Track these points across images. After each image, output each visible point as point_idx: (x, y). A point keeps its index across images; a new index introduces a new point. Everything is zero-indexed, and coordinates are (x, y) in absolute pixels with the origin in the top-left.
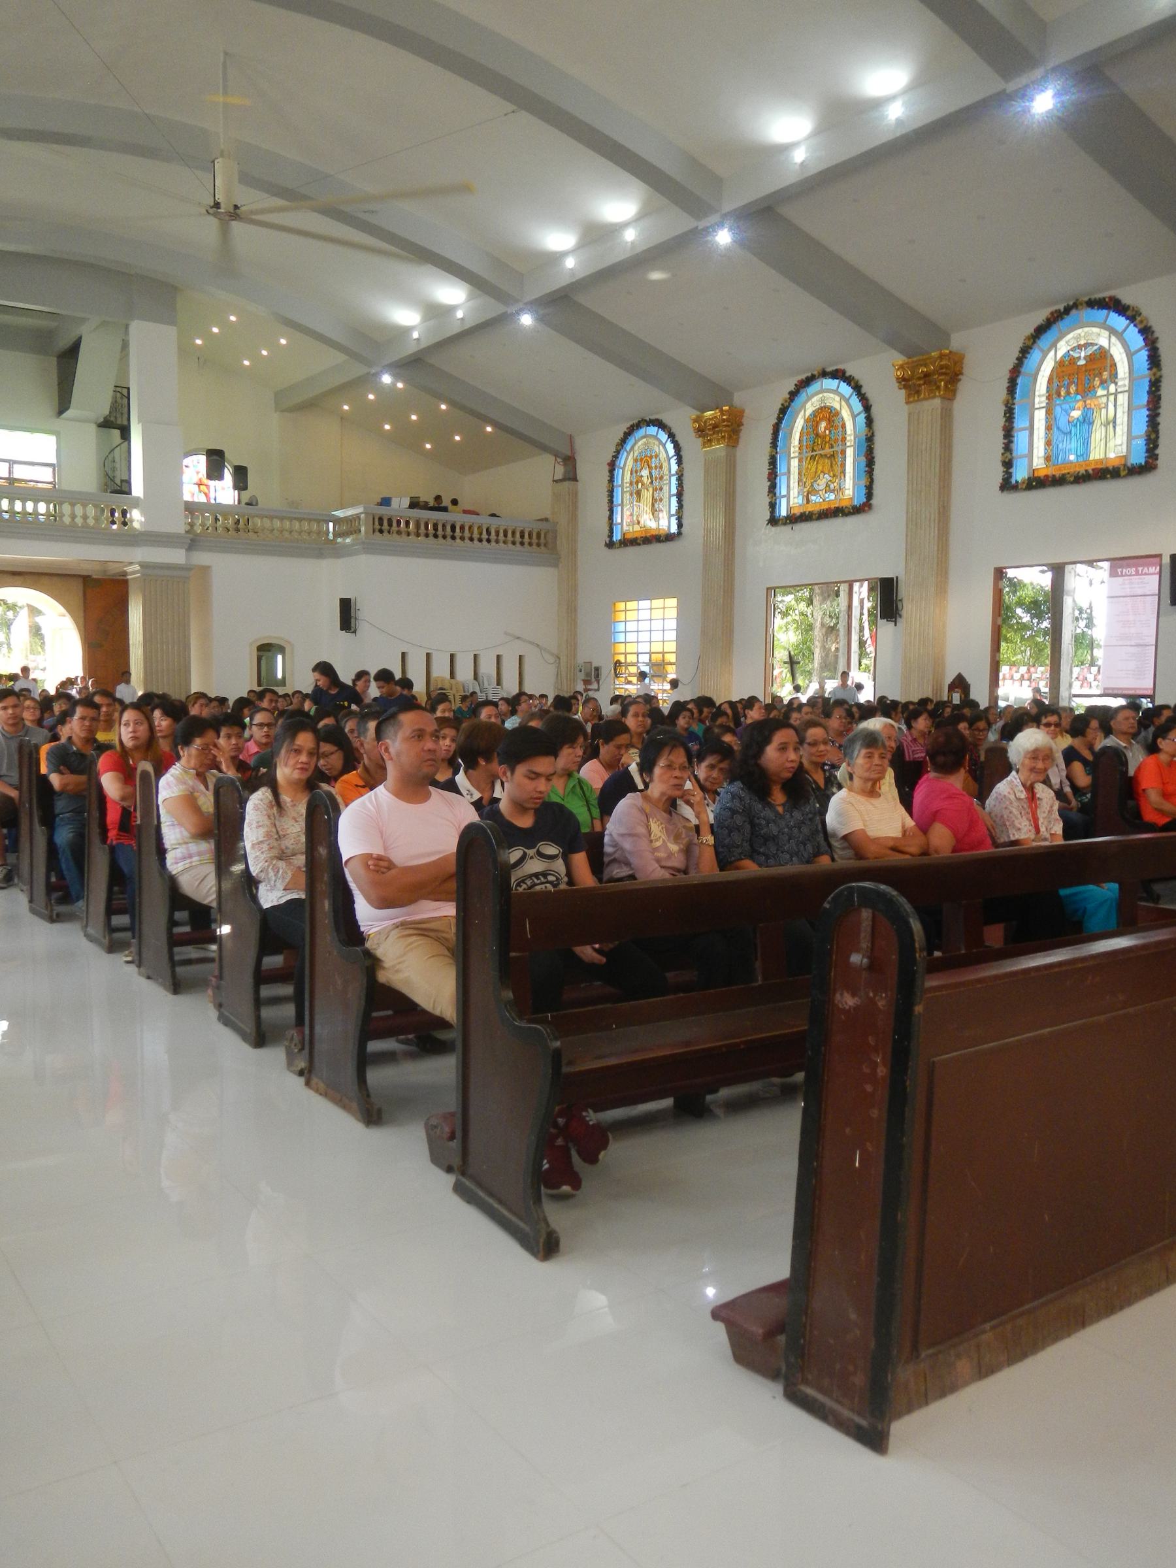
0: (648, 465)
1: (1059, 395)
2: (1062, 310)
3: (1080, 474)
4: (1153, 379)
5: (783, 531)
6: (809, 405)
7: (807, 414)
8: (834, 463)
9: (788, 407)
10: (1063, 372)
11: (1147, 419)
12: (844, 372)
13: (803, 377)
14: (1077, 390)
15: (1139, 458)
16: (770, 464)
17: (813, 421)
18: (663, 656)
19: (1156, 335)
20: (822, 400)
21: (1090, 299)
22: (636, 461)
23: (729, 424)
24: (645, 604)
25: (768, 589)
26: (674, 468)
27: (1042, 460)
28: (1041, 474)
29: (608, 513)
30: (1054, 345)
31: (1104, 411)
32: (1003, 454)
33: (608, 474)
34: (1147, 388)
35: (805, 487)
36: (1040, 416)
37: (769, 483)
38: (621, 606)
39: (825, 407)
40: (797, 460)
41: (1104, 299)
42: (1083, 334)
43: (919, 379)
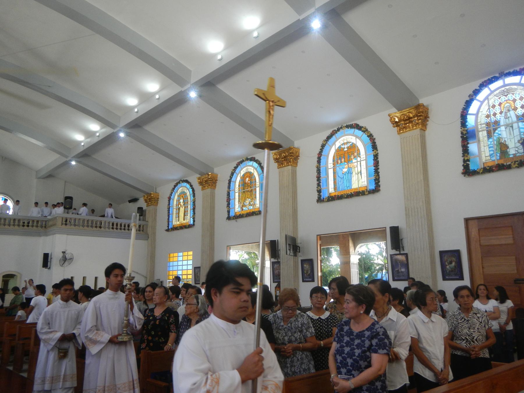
1: (338, 163)
2: (336, 130)
3: (349, 194)
4: (375, 154)
5: (233, 222)
6: (242, 172)
7: (241, 175)
9: (234, 173)
10: (338, 154)
11: (374, 171)
12: (254, 158)
14: (344, 161)
15: (372, 187)
16: (228, 195)
18: (171, 275)
19: (374, 137)
20: (247, 169)
21: (347, 125)
22: (178, 196)
24: (181, 254)
25: (227, 246)
26: (192, 198)
27: (333, 189)
28: (333, 195)
30: (334, 143)
31: (356, 168)
32: (317, 187)
34: (373, 158)
35: (241, 204)
36: (331, 172)
37: (227, 203)
38: (172, 255)
40: (238, 193)
41: (352, 124)
42: (345, 139)
43: (282, 158)
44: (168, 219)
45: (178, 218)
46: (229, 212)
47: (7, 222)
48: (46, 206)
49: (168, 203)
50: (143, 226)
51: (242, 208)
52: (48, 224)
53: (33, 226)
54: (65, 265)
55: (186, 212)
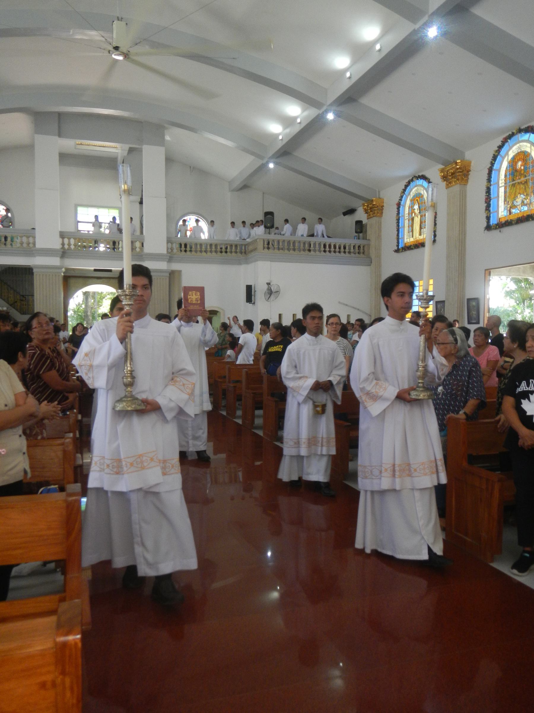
0: (418, 202)
5: (495, 233)
8: (527, 187)
9: (497, 156)
13: (507, 134)
16: (487, 192)
17: (513, 163)
20: (519, 148)
22: (411, 201)
23: (461, 170)
25: (485, 270)
29: (397, 232)
33: (397, 210)
35: (508, 204)
37: (486, 204)
39: (521, 152)
40: (503, 188)
44: (398, 235)
45: (411, 233)
46: (488, 218)
47: (203, 247)
48: (244, 226)
49: (397, 212)
50: (364, 247)
51: (510, 209)
52: (248, 249)
53: (231, 252)
54: (272, 300)
55: (424, 223)
